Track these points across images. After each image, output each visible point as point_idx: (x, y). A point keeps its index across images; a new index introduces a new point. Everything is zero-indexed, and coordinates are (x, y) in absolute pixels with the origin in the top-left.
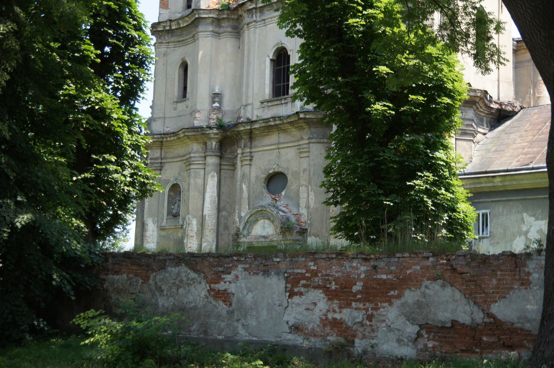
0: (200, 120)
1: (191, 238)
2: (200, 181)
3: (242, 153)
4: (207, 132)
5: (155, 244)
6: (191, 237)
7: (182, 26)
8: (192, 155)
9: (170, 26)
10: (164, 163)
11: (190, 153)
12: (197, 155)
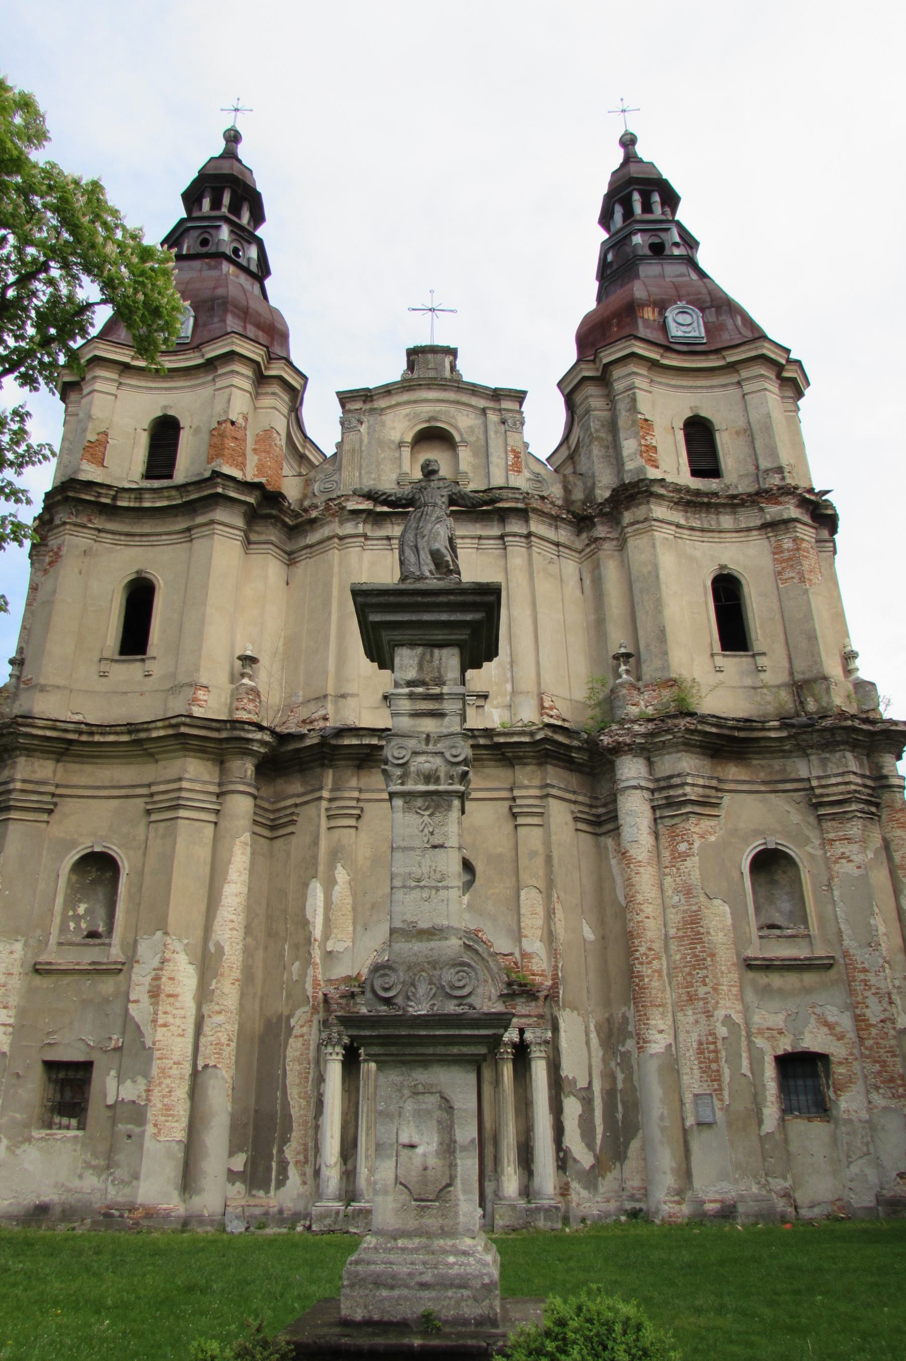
0: (213, 705)
1: (171, 1000)
2: (203, 853)
3: (331, 800)
4: (250, 736)
5: (12, 1012)
6: (169, 996)
7: (147, 504)
8: (185, 784)
9: (114, 498)
10: (60, 796)
11: (180, 779)
12: (198, 787)
